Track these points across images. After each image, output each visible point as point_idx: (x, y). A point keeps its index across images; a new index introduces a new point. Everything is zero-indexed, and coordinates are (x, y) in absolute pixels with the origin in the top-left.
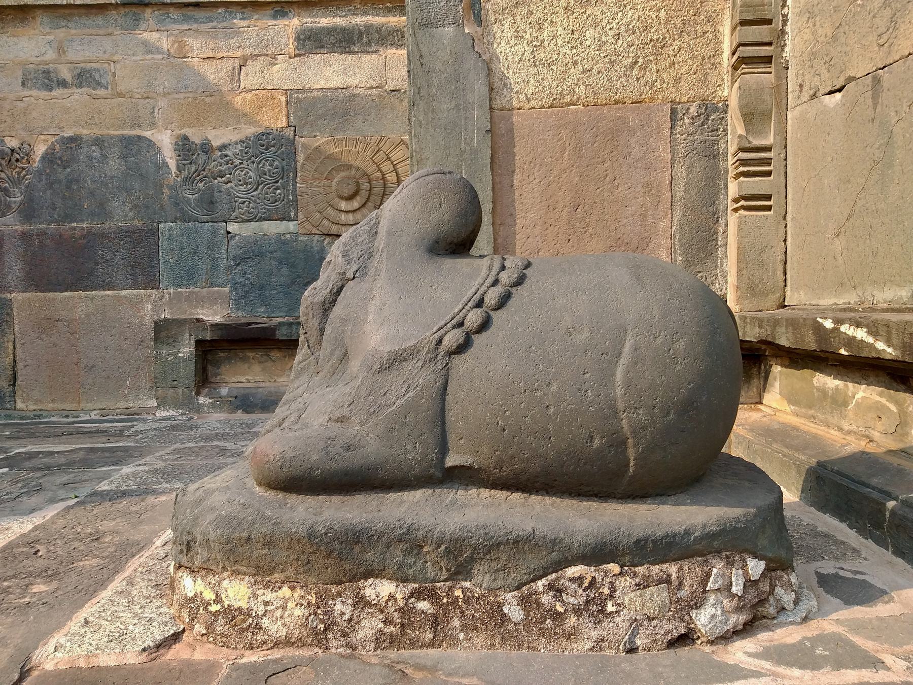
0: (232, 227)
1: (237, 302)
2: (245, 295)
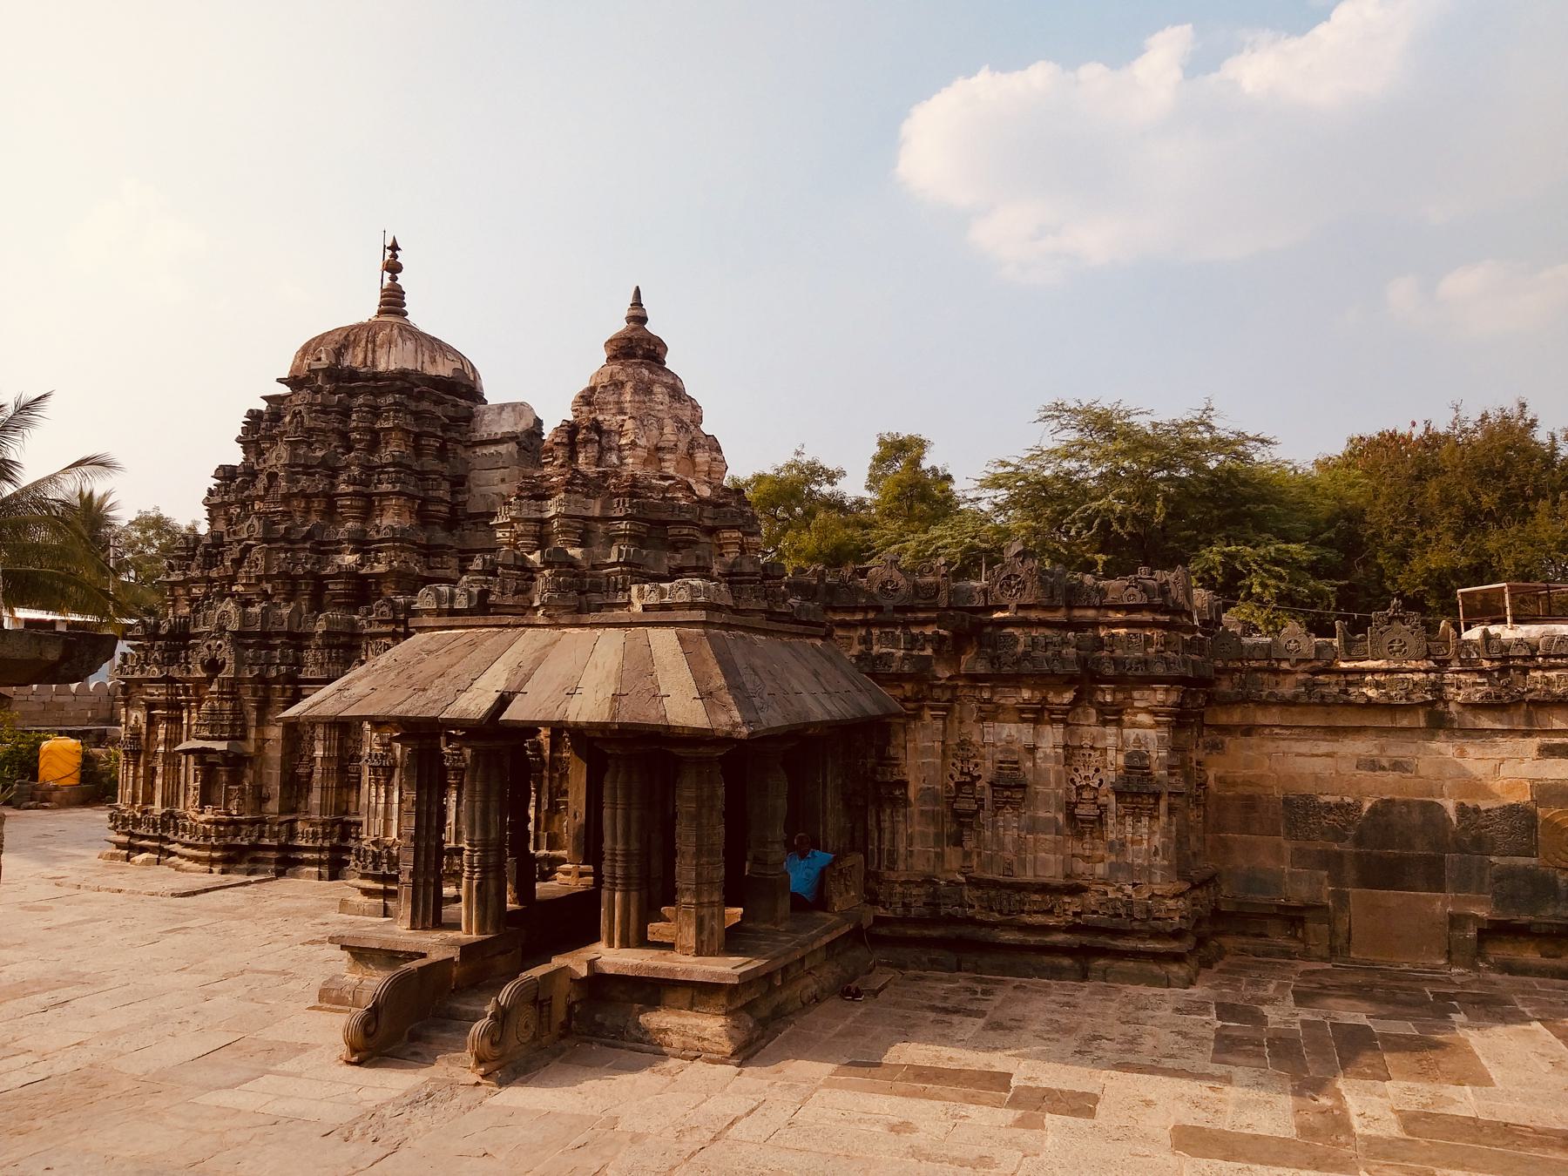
0: (1493, 859)
1: (1497, 906)
2: (1501, 900)
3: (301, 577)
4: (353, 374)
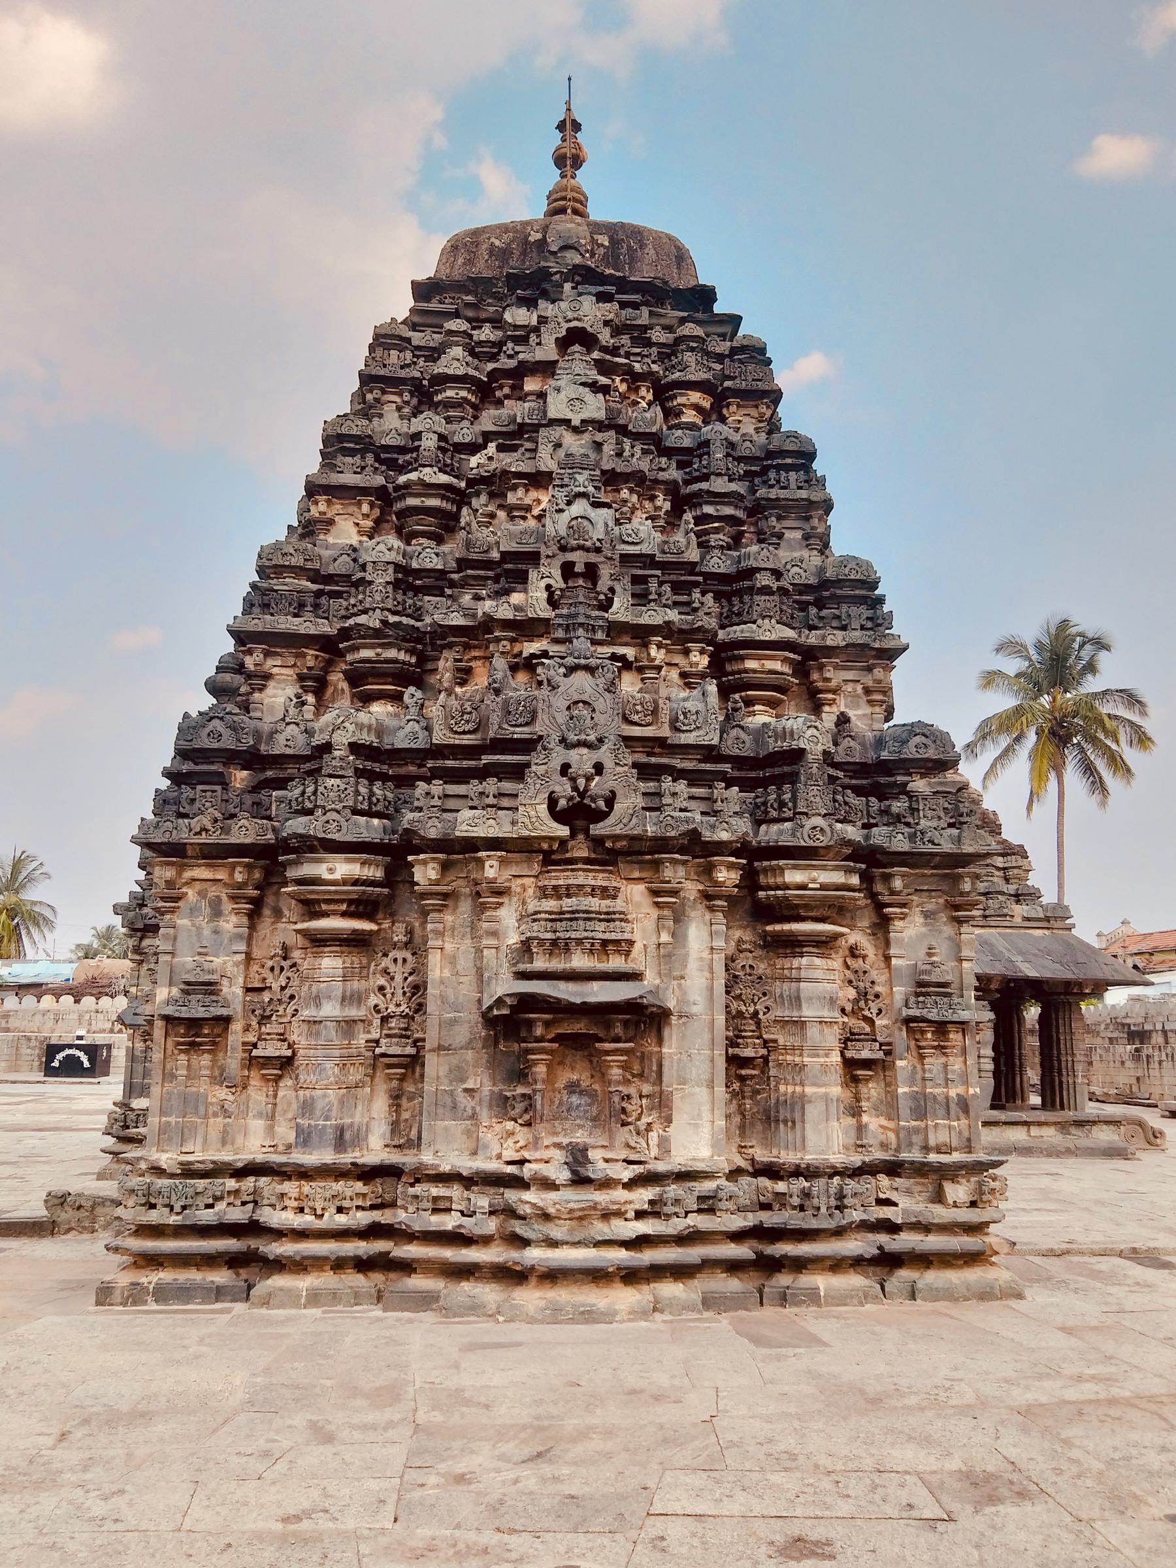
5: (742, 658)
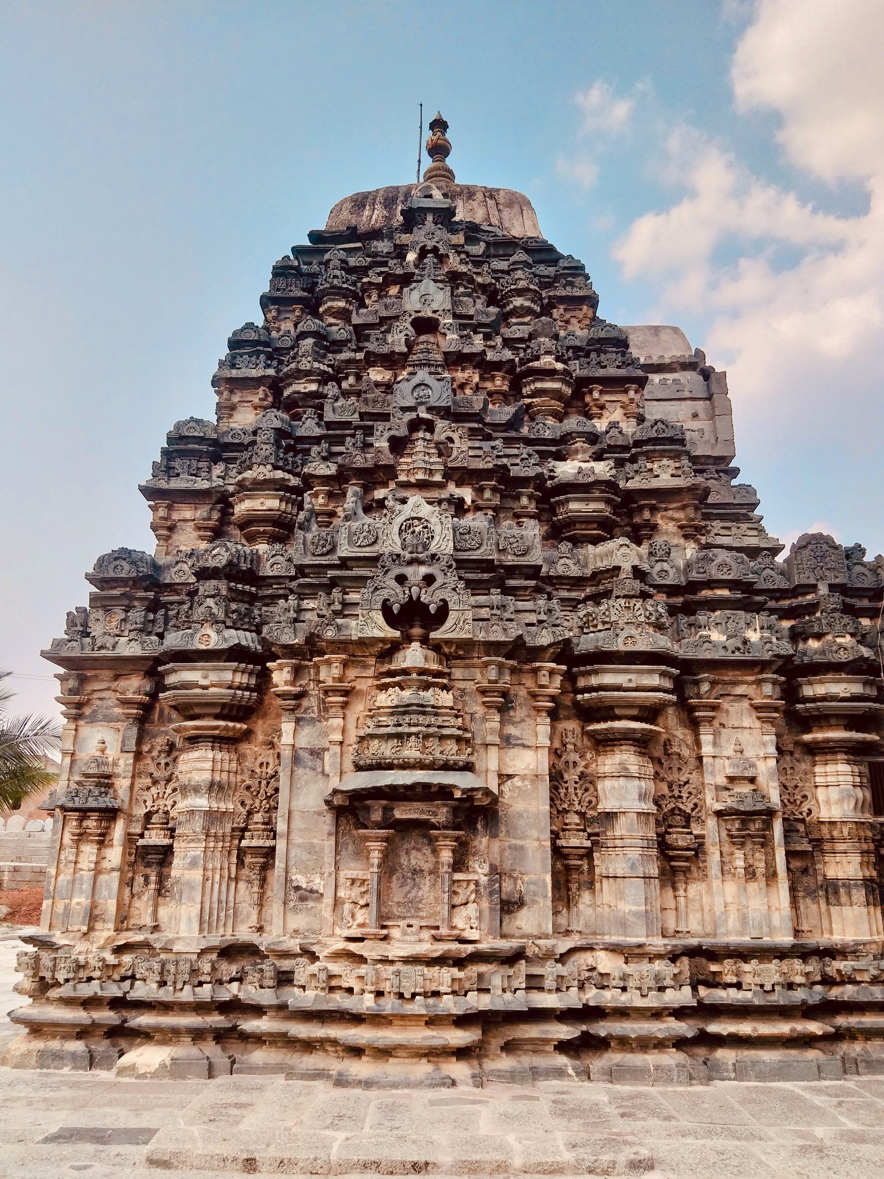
3: (524, 481)
4: (472, 231)
5: (567, 501)
